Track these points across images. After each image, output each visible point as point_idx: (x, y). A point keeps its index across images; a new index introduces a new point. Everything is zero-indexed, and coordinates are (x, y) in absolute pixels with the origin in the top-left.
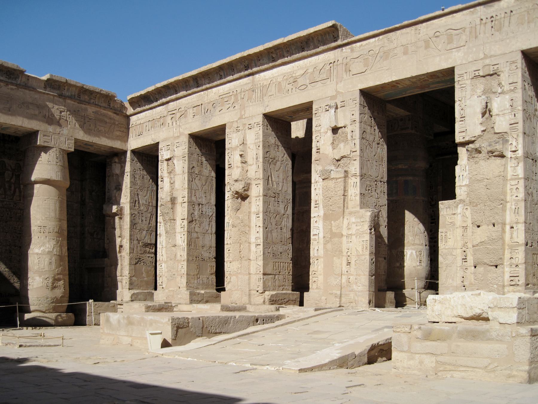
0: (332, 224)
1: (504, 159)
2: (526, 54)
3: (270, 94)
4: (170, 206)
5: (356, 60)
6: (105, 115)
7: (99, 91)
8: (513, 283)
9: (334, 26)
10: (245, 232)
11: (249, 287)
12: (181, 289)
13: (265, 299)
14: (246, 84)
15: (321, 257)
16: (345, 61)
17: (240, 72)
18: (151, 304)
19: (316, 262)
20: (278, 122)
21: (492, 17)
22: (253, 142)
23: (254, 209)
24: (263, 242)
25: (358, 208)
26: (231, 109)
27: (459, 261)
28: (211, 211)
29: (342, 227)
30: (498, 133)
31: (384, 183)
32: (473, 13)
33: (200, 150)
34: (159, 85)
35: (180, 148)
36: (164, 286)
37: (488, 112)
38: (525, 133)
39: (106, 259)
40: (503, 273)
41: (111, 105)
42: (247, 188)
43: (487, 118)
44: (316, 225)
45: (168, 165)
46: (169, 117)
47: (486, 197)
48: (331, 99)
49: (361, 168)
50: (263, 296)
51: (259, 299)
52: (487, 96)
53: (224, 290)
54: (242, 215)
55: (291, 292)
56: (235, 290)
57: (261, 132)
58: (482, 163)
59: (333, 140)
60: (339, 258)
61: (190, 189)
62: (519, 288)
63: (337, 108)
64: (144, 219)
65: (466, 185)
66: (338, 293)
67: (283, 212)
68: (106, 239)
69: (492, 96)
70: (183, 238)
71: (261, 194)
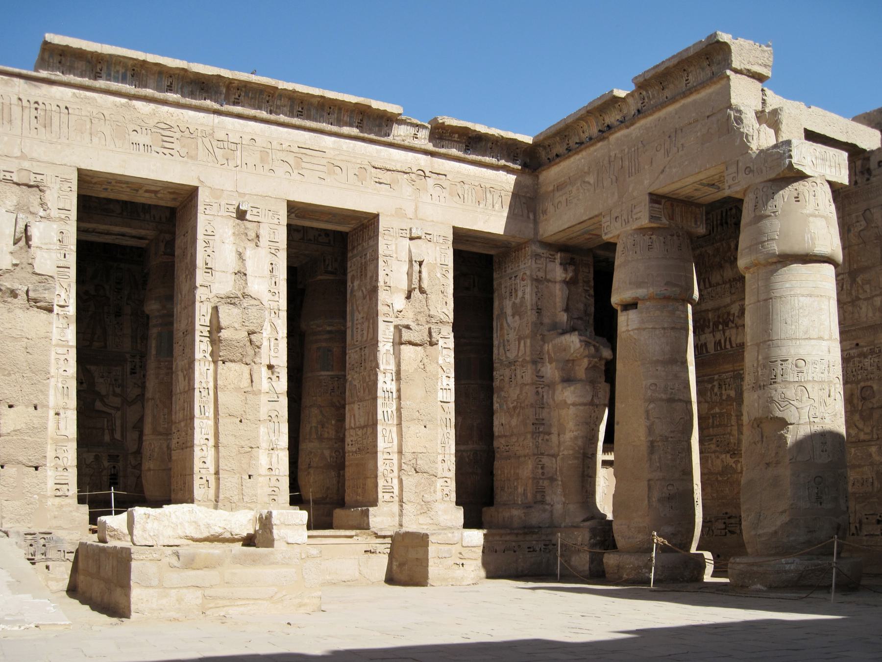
30: (39, 275)
43: (21, 248)
58: (18, 312)
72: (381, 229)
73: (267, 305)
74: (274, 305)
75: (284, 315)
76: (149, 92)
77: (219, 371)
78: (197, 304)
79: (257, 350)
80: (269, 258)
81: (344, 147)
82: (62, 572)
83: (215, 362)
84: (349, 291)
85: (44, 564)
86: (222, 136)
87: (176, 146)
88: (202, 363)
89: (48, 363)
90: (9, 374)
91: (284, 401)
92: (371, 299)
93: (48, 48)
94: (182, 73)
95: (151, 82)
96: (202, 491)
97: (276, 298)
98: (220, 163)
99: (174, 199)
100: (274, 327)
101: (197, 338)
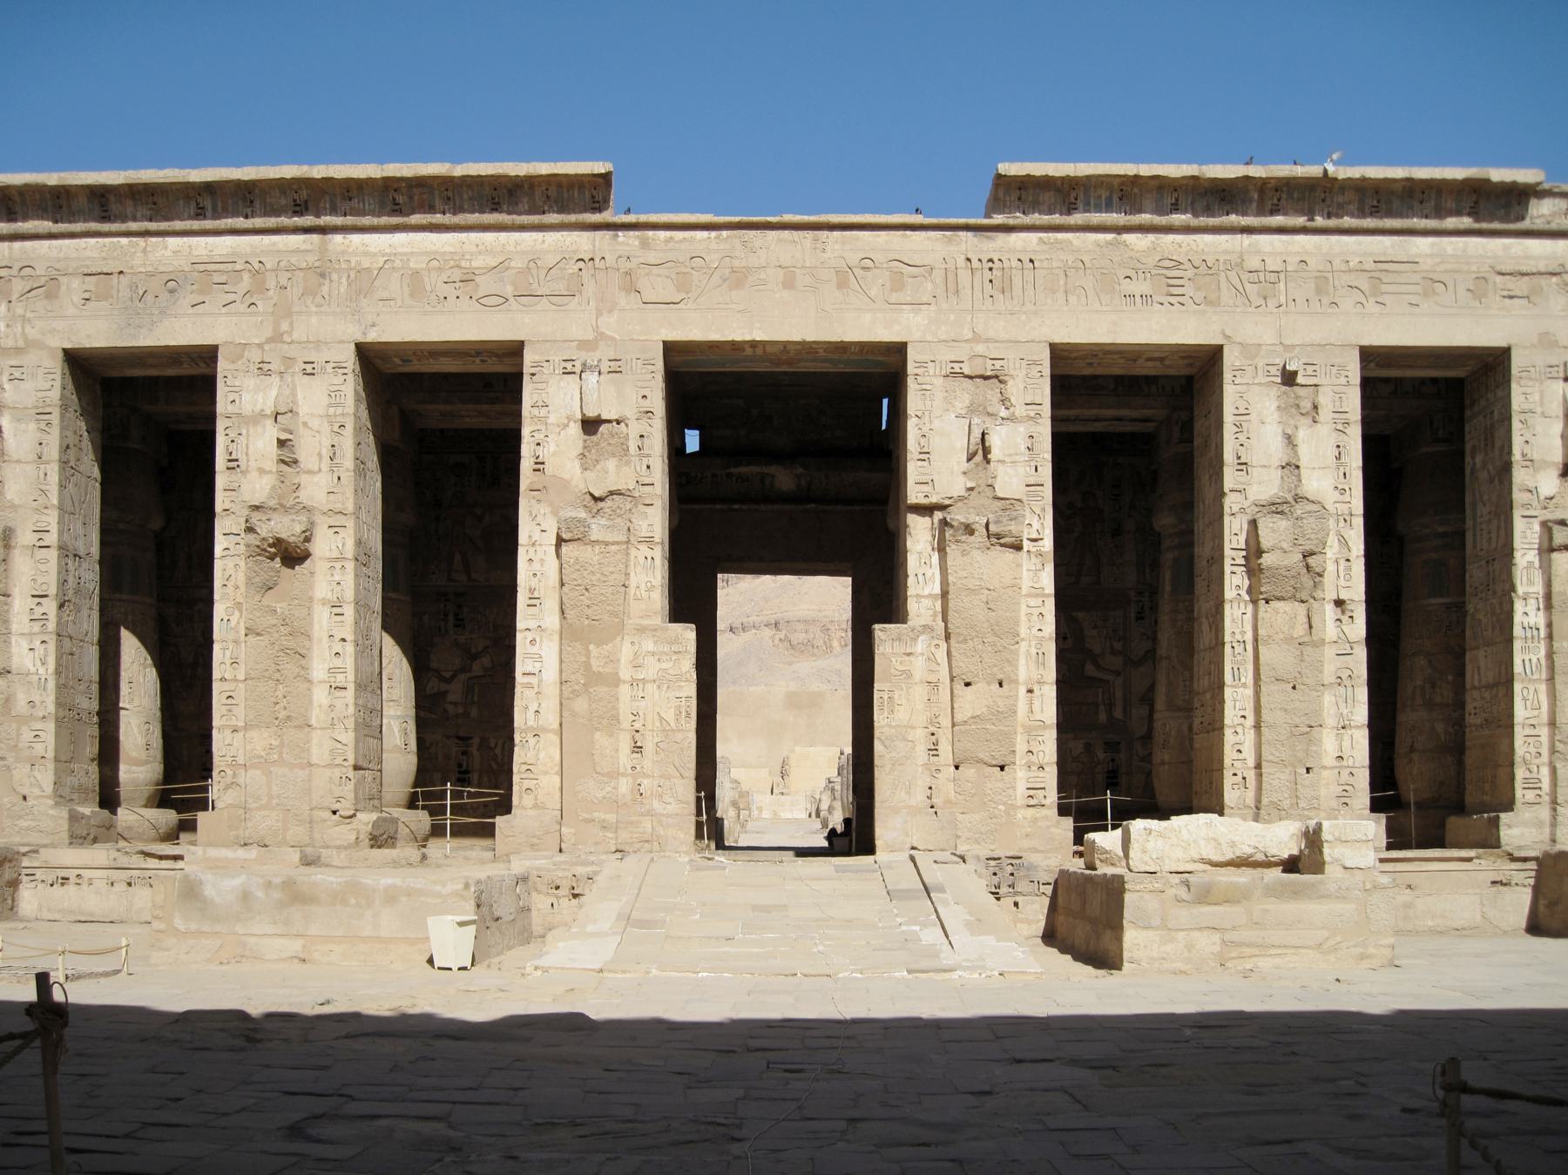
0: (589, 651)
5: (655, 270)
8: (1032, 802)
9: (606, 177)
12: (31, 802)
14: (297, 251)
15: (546, 730)
16: (625, 265)
17: (276, 212)
22: (321, 412)
23: (322, 589)
27: (921, 754)
32: (950, 240)
35: (27, 386)
43: (977, 465)
48: (579, 348)
54: (284, 605)
56: (258, 809)
58: (976, 554)
62: (1044, 812)
72: (1514, 371)
74: (1343, 508)
75: (1359, 522)
76: (1145, 218)
77: (1261, 614)
78: (1227, 519)
81: (1449, 250)
82: (1036, 911)
83: (1254, 602)
84: (1468, 471)
85: (1010, 901)
86: (1254, 263)
87: (1189, 290)
88: (1235, 605)
89: (1017, 623)
90: (965, 641)
91: (1361, 653)
92: (1501, 482)
93: (1001, 181)
94: (1191, 182)
95: (1147, 203)
96: (1237, 793)
99: (1191, 365)
100: (1343, 542)
101: (1228, 569)
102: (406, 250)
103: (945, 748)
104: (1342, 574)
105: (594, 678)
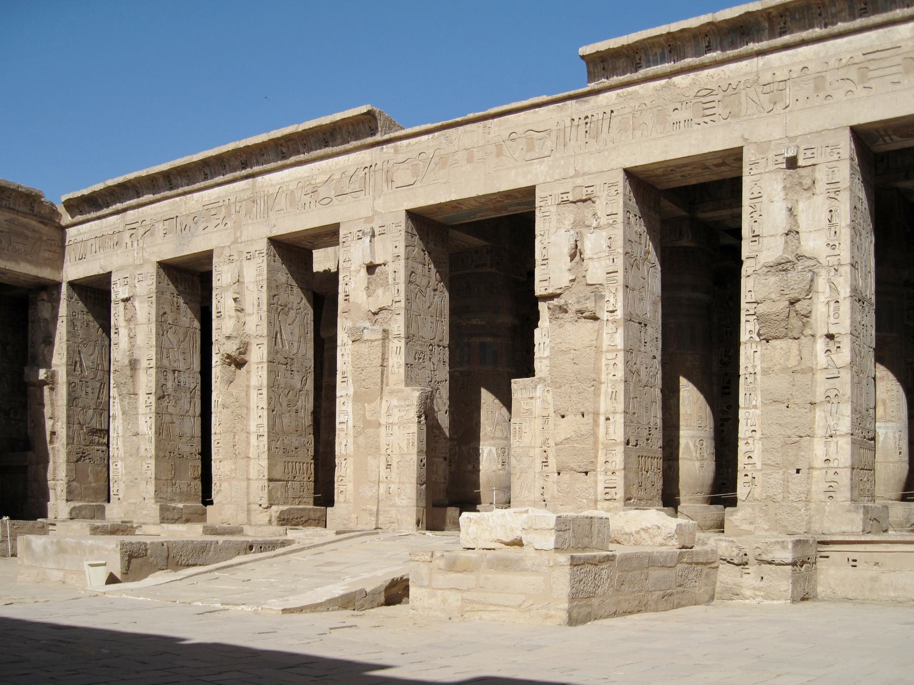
1: (598, 322)
2: (630, 174)
3: (278, 207)
4: (129, 373)
5: (402, 166)
6: (24, 226)
7: (15, 187)
8: (608, 497)
9: (369, 113)
10: (241, 415)
11: (248, 499)
13: (271, 516)
14: (243, 190)
15: (350, 456)
17: (235, 170)
18: (99, 524)
19: (344, 463)
20: (293, 252)
21: (587, 117)
22: (254, 280)
24: (269, 432)
25: (402, 386)
26: (221, 227)
28: (194, 382)
29: (380, 412)
31: (444, 347)
32: (561, 109)
33: (176, 287)
34: (111, 182)
35: (144, 284)
36: (120, 496)
37: (578, 254)
38: (627, 287)
39: (29, 453)
40: (596, 482)
41: (36, 209)
42: (244, 349)
43: (577, 263)
44: (344, 408)
45: (125, 308)
46: (127, 234)
47: (572, 375)
48: (365, 222)
49: (408, 326)
50: (268, 513)
51: (264, 517)
52: (577, 230)
53: (211, 503)
55: (312, 507)
57: (264, 266)
58: (568, 326)
59: (369, 283)
60: (375, 458)
61: (160, 347)
62: (616, 504)
63: (373, 236)
64: (89, 390)
65: (548, 357)
66: (374, 508)
67: (299, 386)
68: (29, 422)
69: (584, 230)
70: (149, 423)
71: (265, 360)
73: (823, 261)
79: (805, 320)
80: (828, 204)
86: (767, 77)
90: (560, 387)
93: (590, 60)
97: (837, 252)
98: (767, 110)
101: (743, 318)
102: (288, 179)
103: (552, 462)
104: (832, 314)
105: (367, 424)
